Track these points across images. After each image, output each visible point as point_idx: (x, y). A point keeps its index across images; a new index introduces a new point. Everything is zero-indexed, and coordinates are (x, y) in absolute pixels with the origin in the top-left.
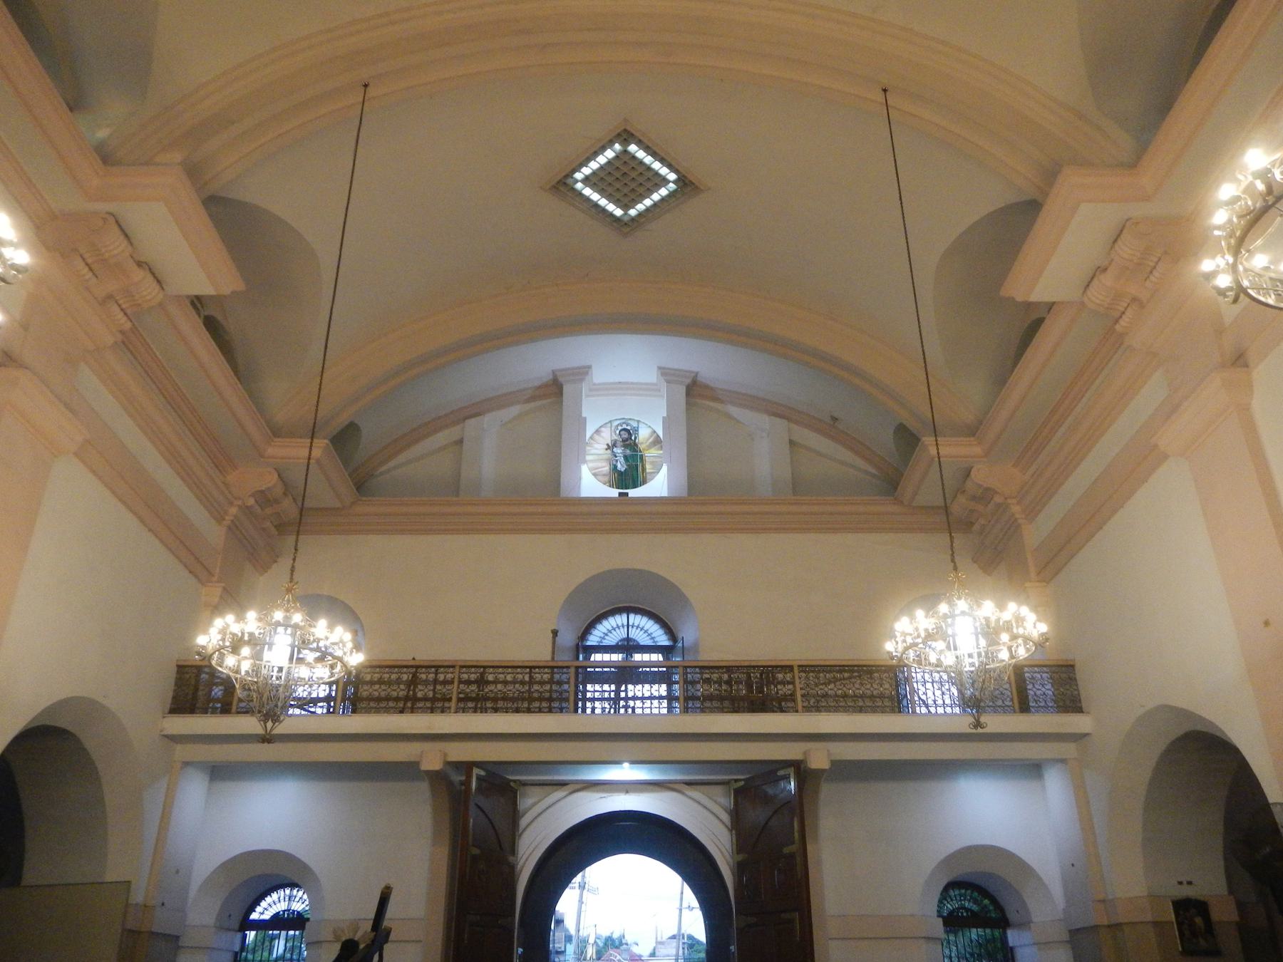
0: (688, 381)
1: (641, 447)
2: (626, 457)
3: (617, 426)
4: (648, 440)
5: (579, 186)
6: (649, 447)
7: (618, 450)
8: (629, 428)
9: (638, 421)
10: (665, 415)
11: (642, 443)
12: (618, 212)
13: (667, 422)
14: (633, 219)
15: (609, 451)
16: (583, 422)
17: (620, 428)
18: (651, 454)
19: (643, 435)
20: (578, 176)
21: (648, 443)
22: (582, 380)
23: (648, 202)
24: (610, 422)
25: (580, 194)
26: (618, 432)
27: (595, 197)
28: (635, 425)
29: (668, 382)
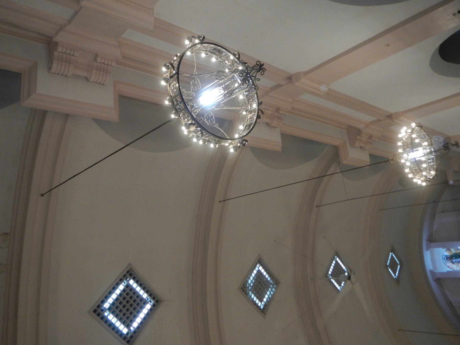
0: (429, 242)
1: (451, 254)
2: (456, 258)
3: (446, 261)
4: (448, 252)
5: (396, 277)
6: (451, 252)
7: (454, 261)
8: (445, 258)
9: (443, 255)
10: (441, 248)
11: (450, 254)
12: (399, 266)
13: (443, 248)
14: (400, 262)
15: (455, 263)
16: (448, 272)
17: (446, 260)
18: (453, 251)
19: (447, 254)
20: (394, 277)
21: (450, 252)
22: (434, 272)
23: (396, 259)
24: (444, 263)
25: (398, 277)
26: (448, 261)
27: (397, 272)
28: (444, 256)
29: (430, 248)
